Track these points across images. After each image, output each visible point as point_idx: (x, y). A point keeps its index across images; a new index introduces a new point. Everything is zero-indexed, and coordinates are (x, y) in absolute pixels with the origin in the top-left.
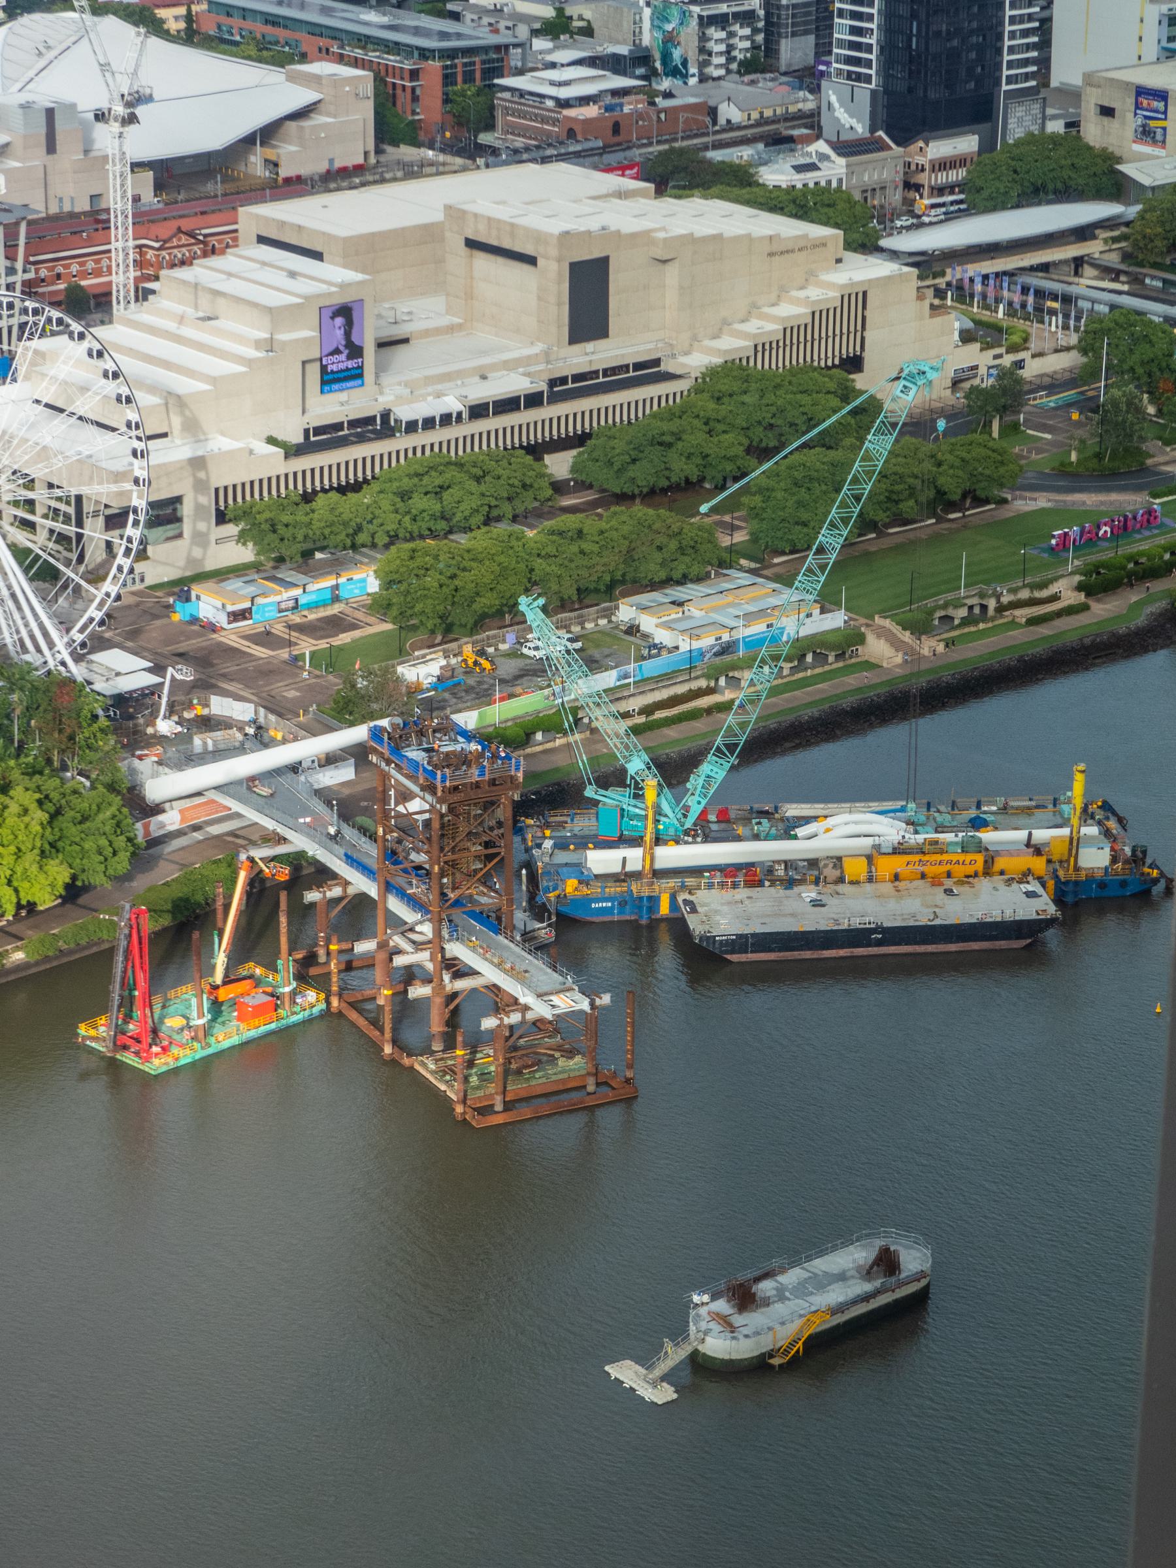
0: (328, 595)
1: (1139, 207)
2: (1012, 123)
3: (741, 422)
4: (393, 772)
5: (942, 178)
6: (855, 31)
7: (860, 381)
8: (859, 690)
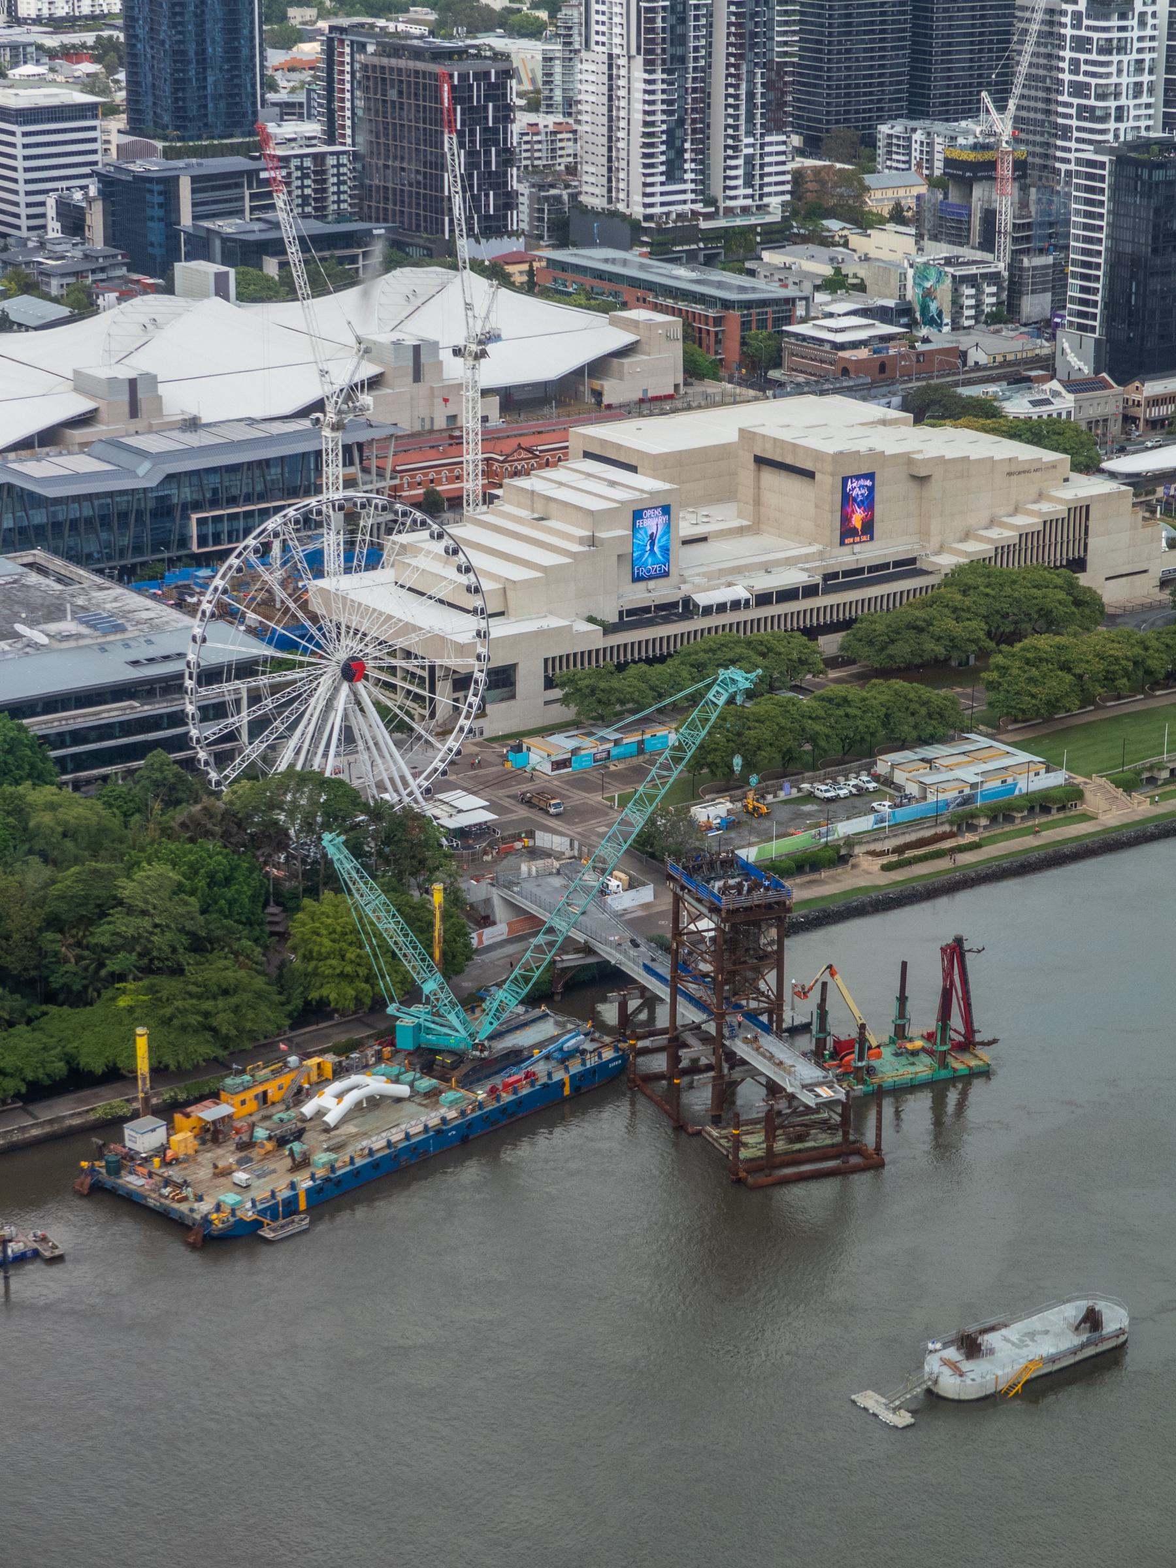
0: (635, 748)
3: (983, 611)
4: (686, 897)
5: (1156, 412)
6: (1084, 290)
7: (1083, 580)
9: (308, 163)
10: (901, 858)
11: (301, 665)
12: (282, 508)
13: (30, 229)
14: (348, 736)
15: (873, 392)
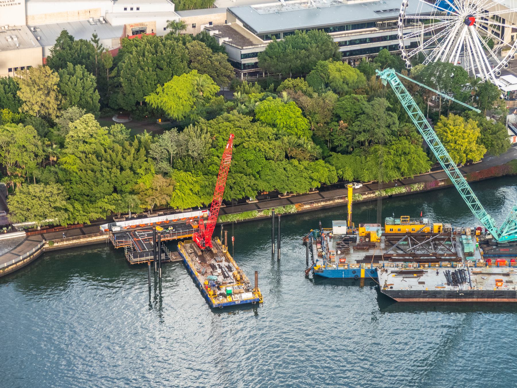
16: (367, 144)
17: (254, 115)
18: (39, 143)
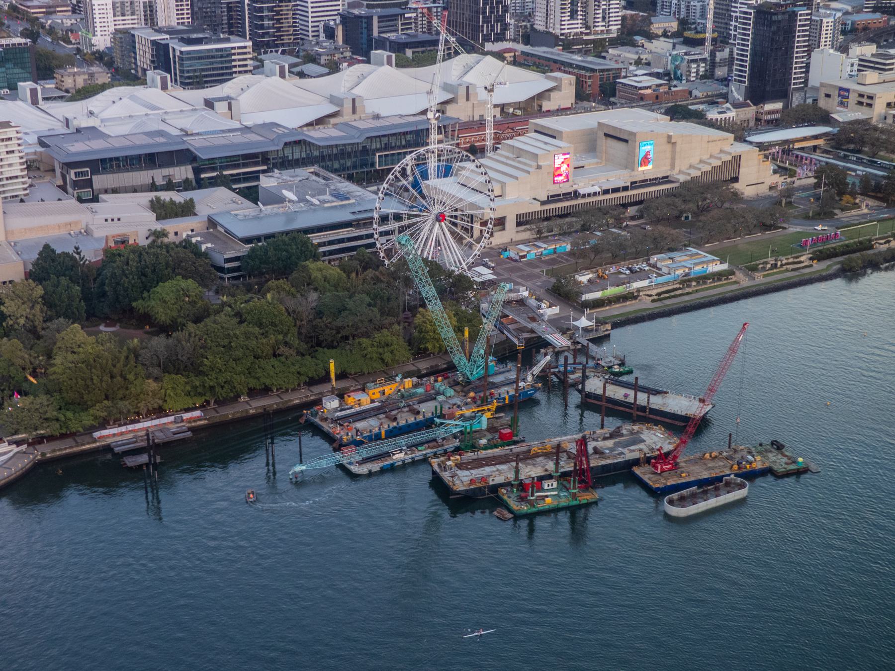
1: (838, 129)
2: (794, 99)
5: (768, 117)
7: (736, 185)
8: (732, 291)
9: (425, 11)
10: (660, 297)
11: (420, 216)
12: (411, 152)
13: (313, 36)
14: (438, 243)
15: (653, 107)
16: (351, 338)
17: (241, 317)
18: (26, 356)
